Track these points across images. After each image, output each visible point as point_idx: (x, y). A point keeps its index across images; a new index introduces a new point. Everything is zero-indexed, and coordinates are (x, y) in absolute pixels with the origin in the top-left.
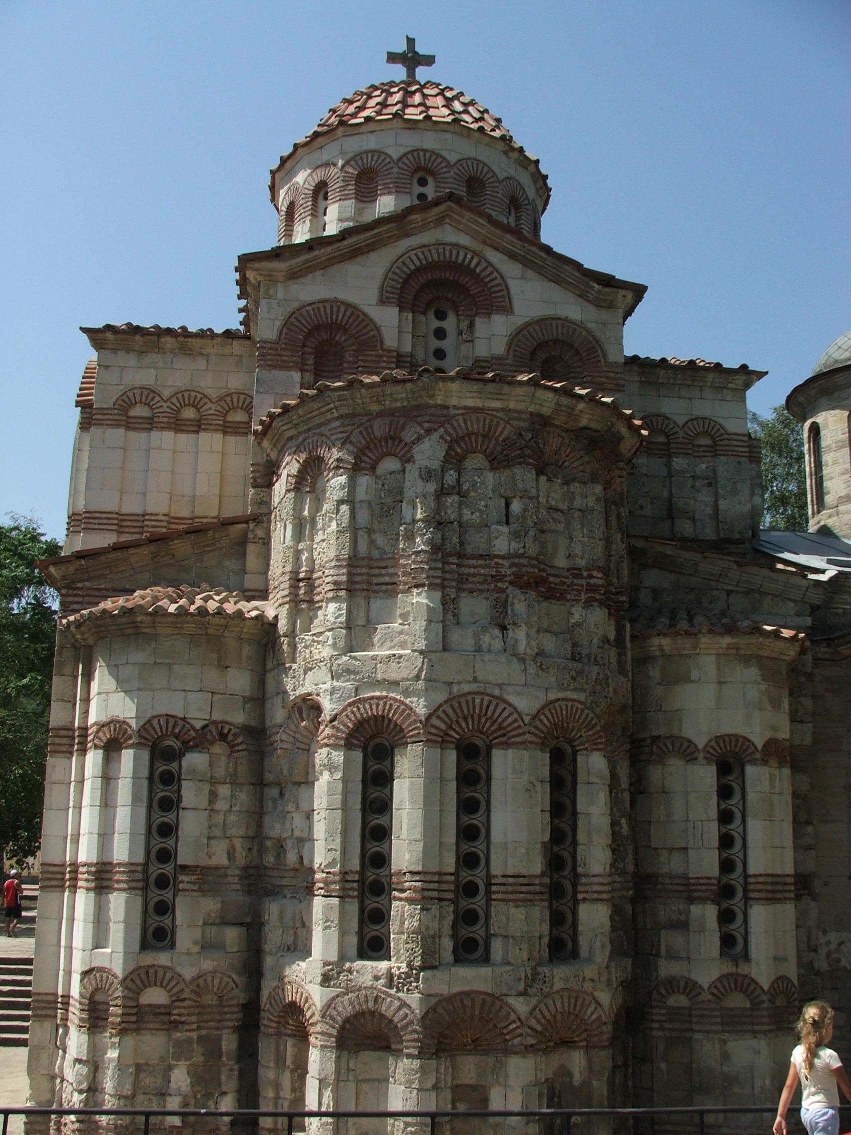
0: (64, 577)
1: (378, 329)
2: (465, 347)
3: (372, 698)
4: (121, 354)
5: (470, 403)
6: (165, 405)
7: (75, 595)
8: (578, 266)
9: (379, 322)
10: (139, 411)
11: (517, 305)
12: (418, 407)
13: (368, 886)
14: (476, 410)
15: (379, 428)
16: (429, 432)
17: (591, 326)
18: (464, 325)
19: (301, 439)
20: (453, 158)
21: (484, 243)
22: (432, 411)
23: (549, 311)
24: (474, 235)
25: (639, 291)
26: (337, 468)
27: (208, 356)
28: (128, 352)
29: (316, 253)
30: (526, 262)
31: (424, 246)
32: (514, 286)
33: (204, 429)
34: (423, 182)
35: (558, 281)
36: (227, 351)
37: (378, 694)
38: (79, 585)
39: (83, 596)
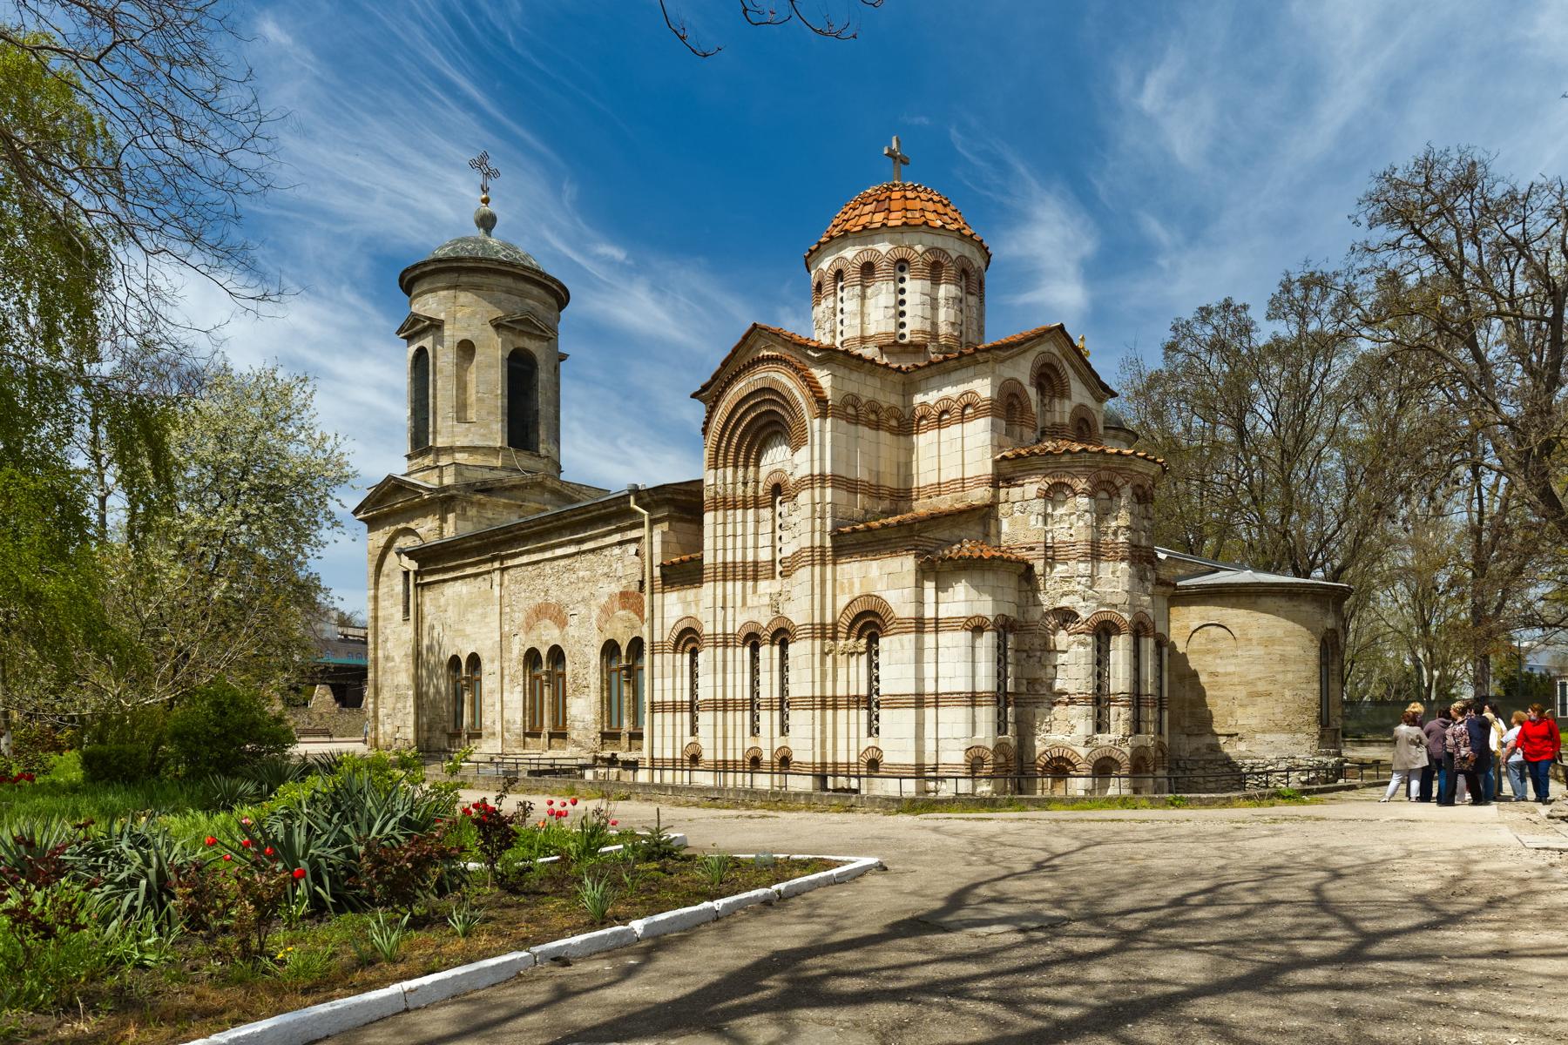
8: (1097, 377)
10: (851, 410)
13: (1100, 700)
30: (1077, 371)
35: (1085, 383)
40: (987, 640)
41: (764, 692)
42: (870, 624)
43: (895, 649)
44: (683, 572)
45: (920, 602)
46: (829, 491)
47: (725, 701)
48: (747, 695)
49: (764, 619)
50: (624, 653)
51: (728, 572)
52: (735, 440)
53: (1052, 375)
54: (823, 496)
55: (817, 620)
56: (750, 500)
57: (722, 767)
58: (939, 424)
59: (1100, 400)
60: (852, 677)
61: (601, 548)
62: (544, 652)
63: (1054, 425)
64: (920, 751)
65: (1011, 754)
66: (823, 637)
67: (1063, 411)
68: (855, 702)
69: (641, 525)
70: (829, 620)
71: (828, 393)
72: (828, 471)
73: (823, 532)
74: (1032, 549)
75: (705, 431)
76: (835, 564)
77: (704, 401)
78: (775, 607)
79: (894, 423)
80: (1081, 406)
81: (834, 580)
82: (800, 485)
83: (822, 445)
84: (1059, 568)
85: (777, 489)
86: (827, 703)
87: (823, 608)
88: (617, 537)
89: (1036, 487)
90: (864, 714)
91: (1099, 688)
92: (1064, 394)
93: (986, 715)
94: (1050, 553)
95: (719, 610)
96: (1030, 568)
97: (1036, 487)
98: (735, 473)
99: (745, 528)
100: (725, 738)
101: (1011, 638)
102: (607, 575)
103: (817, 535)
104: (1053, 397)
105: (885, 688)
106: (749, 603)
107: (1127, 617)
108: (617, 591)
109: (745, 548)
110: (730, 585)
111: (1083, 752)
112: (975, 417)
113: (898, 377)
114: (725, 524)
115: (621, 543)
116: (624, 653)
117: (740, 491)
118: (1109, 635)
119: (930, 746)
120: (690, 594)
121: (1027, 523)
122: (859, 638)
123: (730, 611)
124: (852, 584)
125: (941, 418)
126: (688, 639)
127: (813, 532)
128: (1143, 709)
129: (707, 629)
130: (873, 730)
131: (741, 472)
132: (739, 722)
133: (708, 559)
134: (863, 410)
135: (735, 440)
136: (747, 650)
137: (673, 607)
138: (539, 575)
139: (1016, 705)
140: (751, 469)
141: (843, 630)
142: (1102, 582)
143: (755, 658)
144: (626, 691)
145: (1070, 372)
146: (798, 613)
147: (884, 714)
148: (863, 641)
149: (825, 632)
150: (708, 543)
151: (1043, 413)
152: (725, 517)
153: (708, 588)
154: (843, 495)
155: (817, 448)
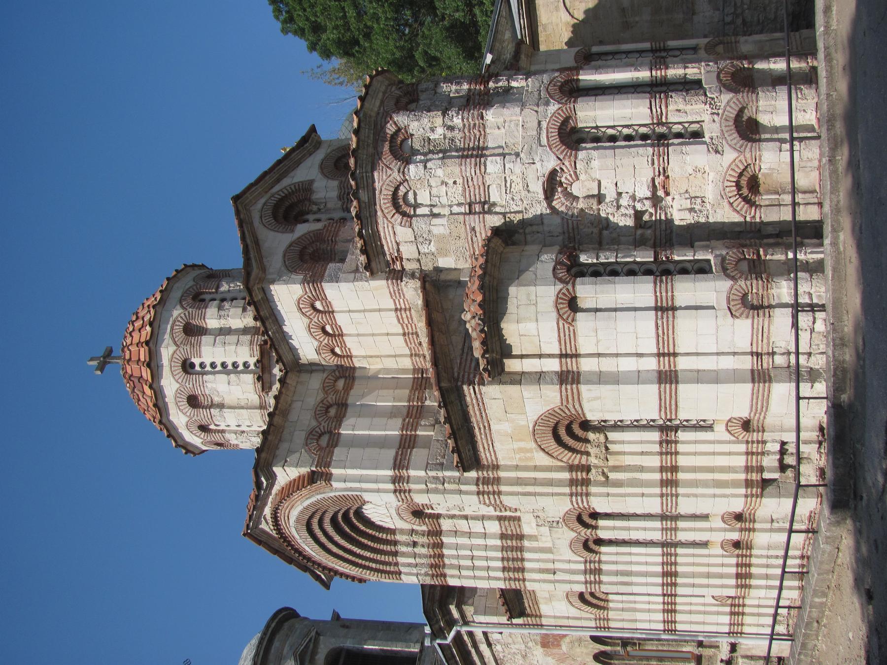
0: (450, 381)
1: (309, 232)
2: (329, 205)
3: (547, 137)
4: (278, 452)
5: (378, 103)
6: (323, 424)
7: (463, 376)
9: (306, 231)
11: (309, 178)
12: (376, 125)
13: (659, 138)
14: (382, 102)
17: (329, 151)
18: (315, 208)
19: (379, 213)
20: (191, 283)
21: (266, 192)
22: (379, 118)
23: (317, 166)
25: (313, 129)
26: (403, 172)
27: (292, 401)
28: (277, 448)
29: (252, 256)
31: (261, 217)
32: (296, 180)
33: (346, 400)
34: (203, 300)
35: (298, 163)
36: (292, 389)
37: (545, 131)
38: (456, 375)
39: (464, 372)
40: (588, 292)
41: (657, 536)
42: (570, 432)
43: (596, 403)
45: (539, 377)
46: (412, 473)
47: (665, 574)
49: (567, 534)
52: (368, 554)
53: (287, 204)
54: (418, 480)
55: (567, 490)
56: (432, 540)
57: (743, 577)
58: (338, 335)
59: (319, 144)
60: (638, 450)
63: (340, 198)
64: (734, 377)
66: (586, 482)
67: (326, 190)
68: (668, 446)
69: (471, 634)
70: (566, 475)
71: (304, 470)
72: (390, 473)
73: (459, 481)
74: (473, 229)
76: (496, 467)
77: (331, 578)
78: (552, 525)
79: (341, 383)
80: (322, 167)
81: (517, 468)
83: (361, 479)
84: (495, 197)
85: (418, 513)
86: (670, 477)
87: (550, 483)
88: (483, 647)
89: (398, 229)
90: (682, 435)
92: (307, 188)
93: (686, 290)
94: (477, 208)
95: (557, 577)
96: (496, 231)
97: (398, 229)
98: (404, 554)
99: (464, 547)
100: (708, 575)
101: (584, 258)
102: (524, 657)
103: (464, 488)
104: (310, 200)
106: (549, 545)
108: (541, 650)
109: (486, 548)
111: (730, 156)
112: (324, 299)
113: (291, 380)
114: (459, 568)
115: (489, 645)
117: (424, 551)
118: (575, 130)
119: (727, 363)
121: (441, 238)
122: (587, 441)
123: (558, 565)
124: (521, 450)
125: (330, 335)
127: (460, 492)
131: (403, 549)
132: (690, 560)
133: (501, 585)
135: (368, 554)
136: (603, 549)
140: (398, 537)
141: (576, 459)
142: (510, 141)
143: (610, 542)
145: (286, 182)
146: (560, 505)
147: (683, 415)
148: (591, 436)
149: (580, 480)
151: (328, 211)
152: (452, 566)
153: (530, 586)
154: (418, 455)
155: (365, 486)
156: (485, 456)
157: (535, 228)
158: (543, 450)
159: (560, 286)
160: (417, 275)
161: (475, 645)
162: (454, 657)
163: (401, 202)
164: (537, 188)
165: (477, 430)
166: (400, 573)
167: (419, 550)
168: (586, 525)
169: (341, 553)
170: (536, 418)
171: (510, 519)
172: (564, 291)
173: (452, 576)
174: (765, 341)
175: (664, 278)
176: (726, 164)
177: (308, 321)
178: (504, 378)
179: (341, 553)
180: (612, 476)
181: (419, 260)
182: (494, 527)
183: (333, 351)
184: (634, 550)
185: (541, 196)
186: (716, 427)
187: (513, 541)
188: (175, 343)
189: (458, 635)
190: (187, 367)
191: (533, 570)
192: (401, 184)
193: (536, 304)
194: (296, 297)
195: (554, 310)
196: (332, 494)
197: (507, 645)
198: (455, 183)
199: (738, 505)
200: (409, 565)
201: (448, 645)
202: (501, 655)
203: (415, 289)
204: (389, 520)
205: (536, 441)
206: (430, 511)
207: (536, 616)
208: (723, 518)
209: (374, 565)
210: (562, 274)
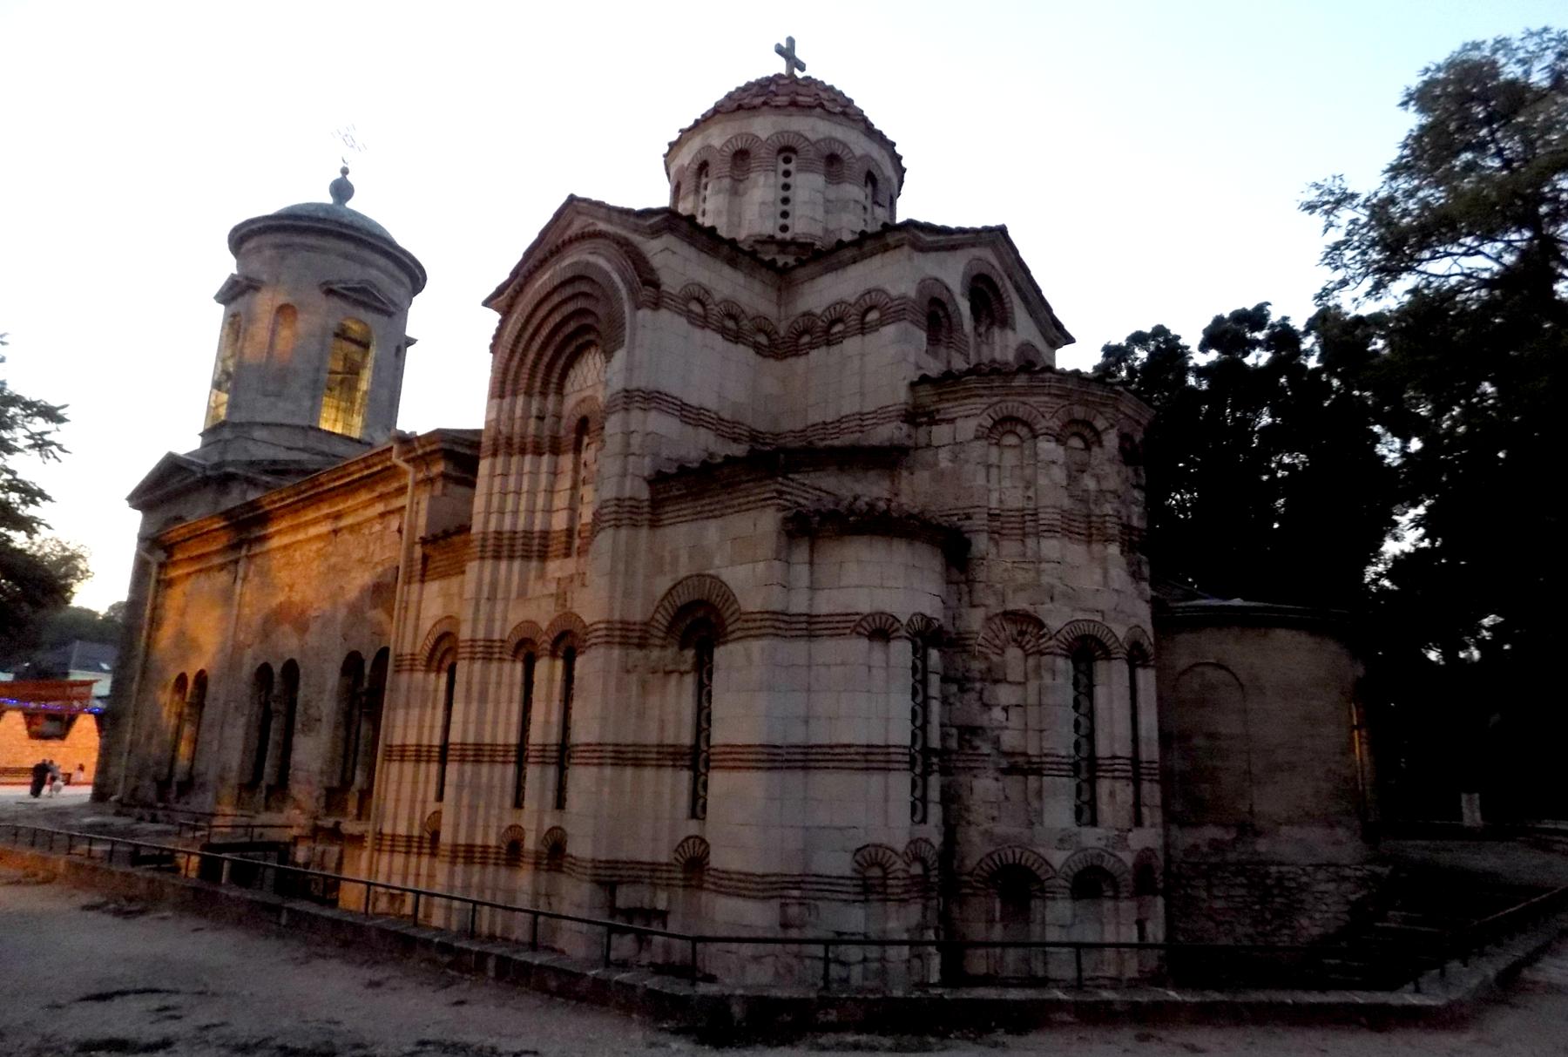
5: (1130, 412)
10: (696, 307)
11: (1018, 327)
15: (1079, 412)
16: (1112, 426)
18: (982, 329)
19: (995, 399)
24: (1002, 262)
25: (1070, 340)
41: (535, 736)
44: (444, 546)
48: (513, 739)
49: (543, 614)
50: (367, 670)
51: (502, 547)
56: (546, 443)
57: (468, 854)
59: (1055, 345)
61: (359, 524)
62: (277, 669)
63: (993, 361)
65: (931, 857)
67: (1004, 346)
68: (671, 756)
69: (401, 491)
74: (968, 517)
75: (493, 348)
77: (497, 310)
78: (561, 597)
79: (762, 339)
82: (609, 410)
85: (583, 426)
86: (626, 757)
88: (380, 508)
90: (685, 776)
91: (1077, 745)
92: (1005, 322)
98: (527, 405)
101: (934, 654)
102: (361, 561)
104: (992, 324)
105: (719, 736)
107: (1121, 632)
110: (503, 565)
111: (1058, 858)
112: (882, 323)
114: (505, 475)
115: (382, 515)
116: (367, 670)
120: (454, 583)
122: (682, 647)
123: (500, 607)
124: (675, 559)
126: (444, 651)
128: (1146, 786)
129: (465, 633)
130: (698, 808)
133: (476, 528)
134: (715, 310)
135: (531, 356)
136: (519, 667)
137: (432, 603)
138: (288, 564)
139: (945, 771)
140: (552, 399)
144: (365, 728)
146: (591, 607)
148: (690, 654)
149: (629, 636)
150: (479, 503)
152: (507, 466)
153: (472, 567)
156: (669, 511)
157: (966, 598)
158: (674, 587)
159: (904, 621)
160: (910, 443)
161: (381, 497)
162: (368, 467)
163: (1008, 427)
164: (1019, 603)
165: (707, 501)
166: (502, 397)
167: (532, 423)
168: (556, 643)
169: (535, 322)
170: (724, 578)
171: (572, 542)
172: (897, 625)
173: (493, 466)
174: (819, 894)
175: (907, 758)
176: (1041, 851)
177: (852, 300)
178: (784, 539)
179: (535, 322)
180: (634, 677)
181: (929, 446)
182: (559, 522)
183: (805, 331)
184: (516, 708)
185: (1011, 607)
186: (693, 823)
187: (535, 547)
188: (818, 141)
189: (405, 473)
190: (787, 152)
191: (495, 571)
192: (1032, 430)
193: (882, 587)
194: (888, 287)
195: (874, 610)
196: (627, 309)
197: (380, 537)
198: (1029, 498)
199: (580, 847)
200: (512, 410)
201: (390, 459)
202: (366, 531)
203: (890, 439)
204: (577, 387)
205: (687, 578)
206: (586, 440)
207: (423, 575)
208: (559, 828)
209: (515, 363)
210: (918, 624)
